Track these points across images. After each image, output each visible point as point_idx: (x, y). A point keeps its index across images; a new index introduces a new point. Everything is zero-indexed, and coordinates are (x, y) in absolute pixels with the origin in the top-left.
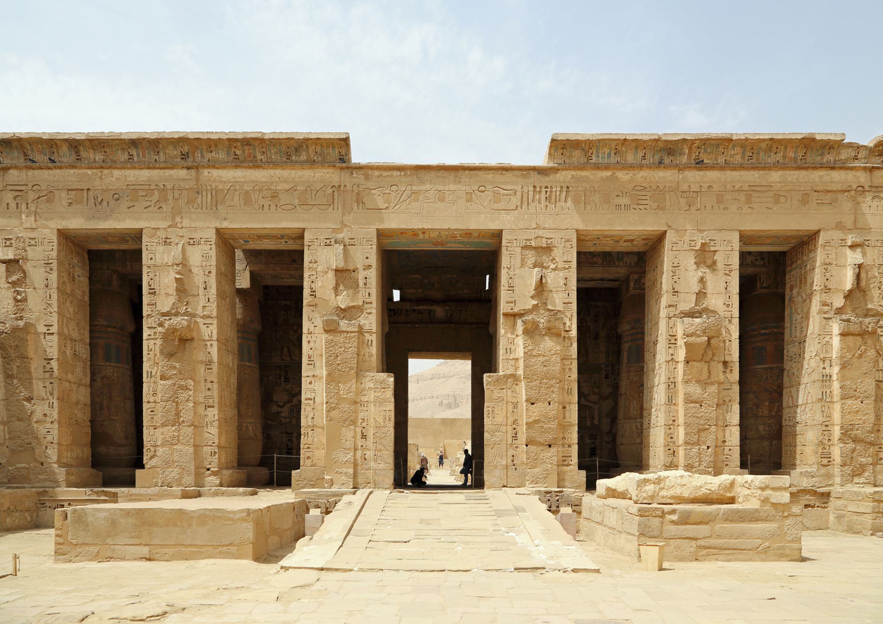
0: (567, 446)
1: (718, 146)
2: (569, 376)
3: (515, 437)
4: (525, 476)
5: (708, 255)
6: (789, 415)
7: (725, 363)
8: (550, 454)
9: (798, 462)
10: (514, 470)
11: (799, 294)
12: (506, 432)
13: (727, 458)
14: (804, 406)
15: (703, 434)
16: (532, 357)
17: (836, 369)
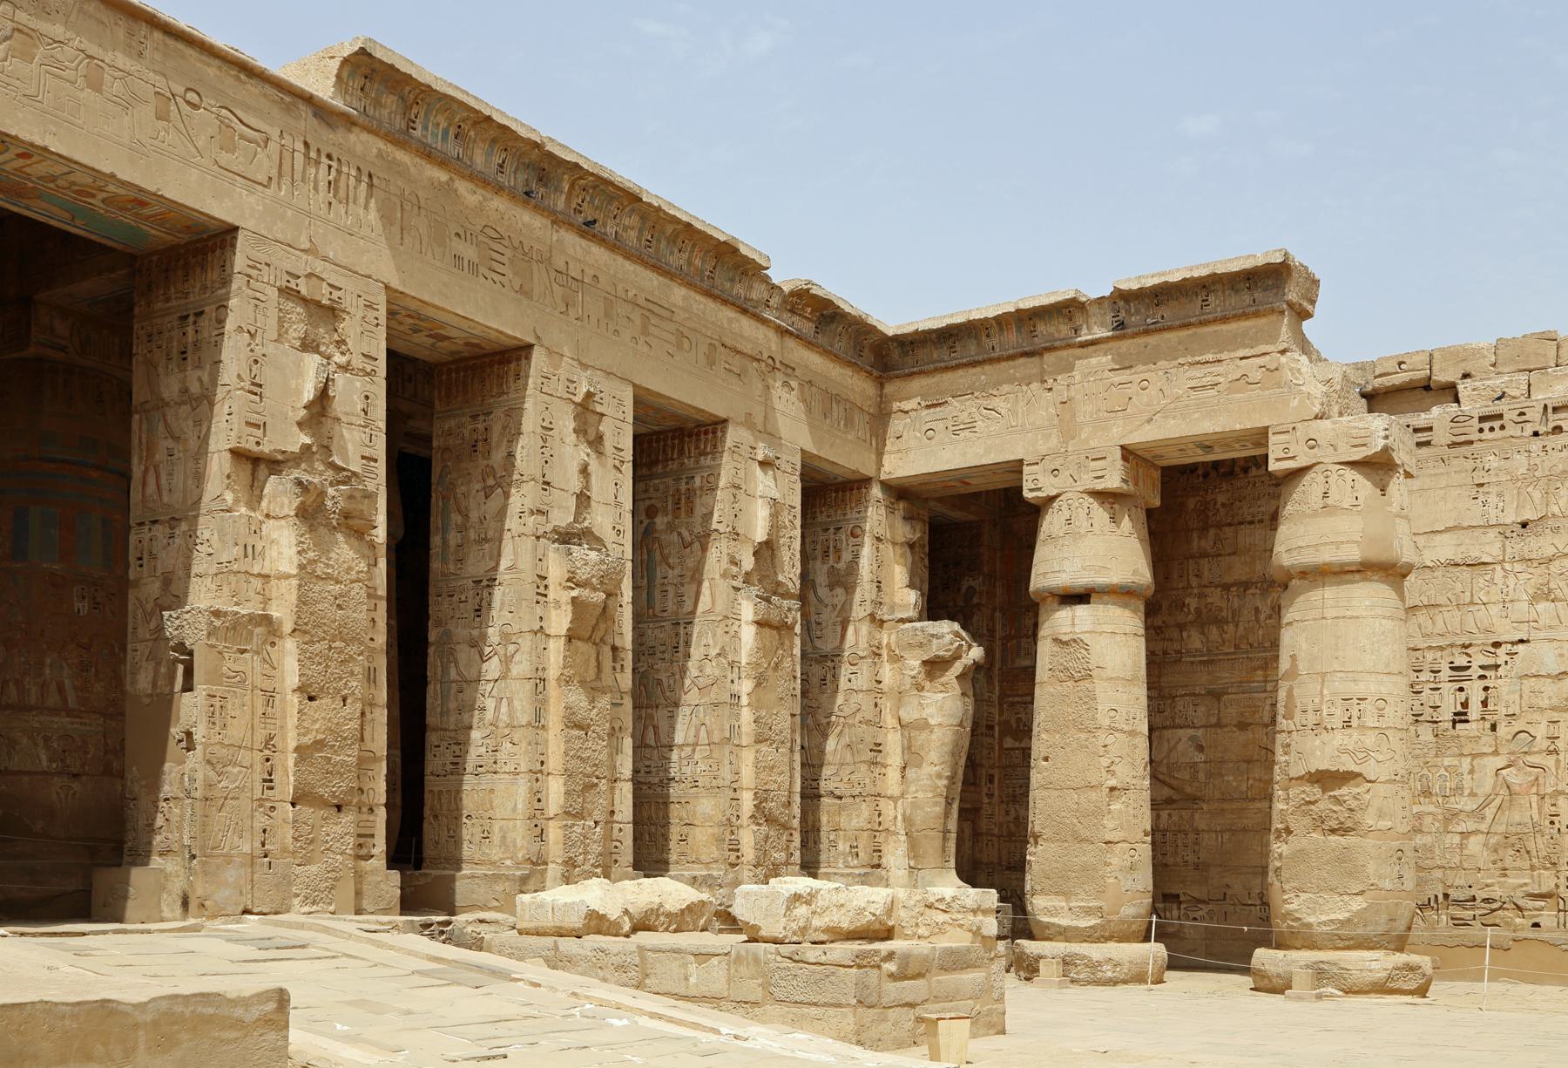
0: (365, 809)
1: (611, 199)
2: (372, 639)
3: (268, 782)
4: (290, 884)
5: (592, 419)
6: (647, 763)
7: (614, 649)
8: (338, 829)
9: (673, 857)
10: (266, 869)
11: (671, 527)
12: (252, 766)
13: (616, 847)
14: (688, 750)
15: (589, 796)
16: (314, 580)
17: (746, 686)
